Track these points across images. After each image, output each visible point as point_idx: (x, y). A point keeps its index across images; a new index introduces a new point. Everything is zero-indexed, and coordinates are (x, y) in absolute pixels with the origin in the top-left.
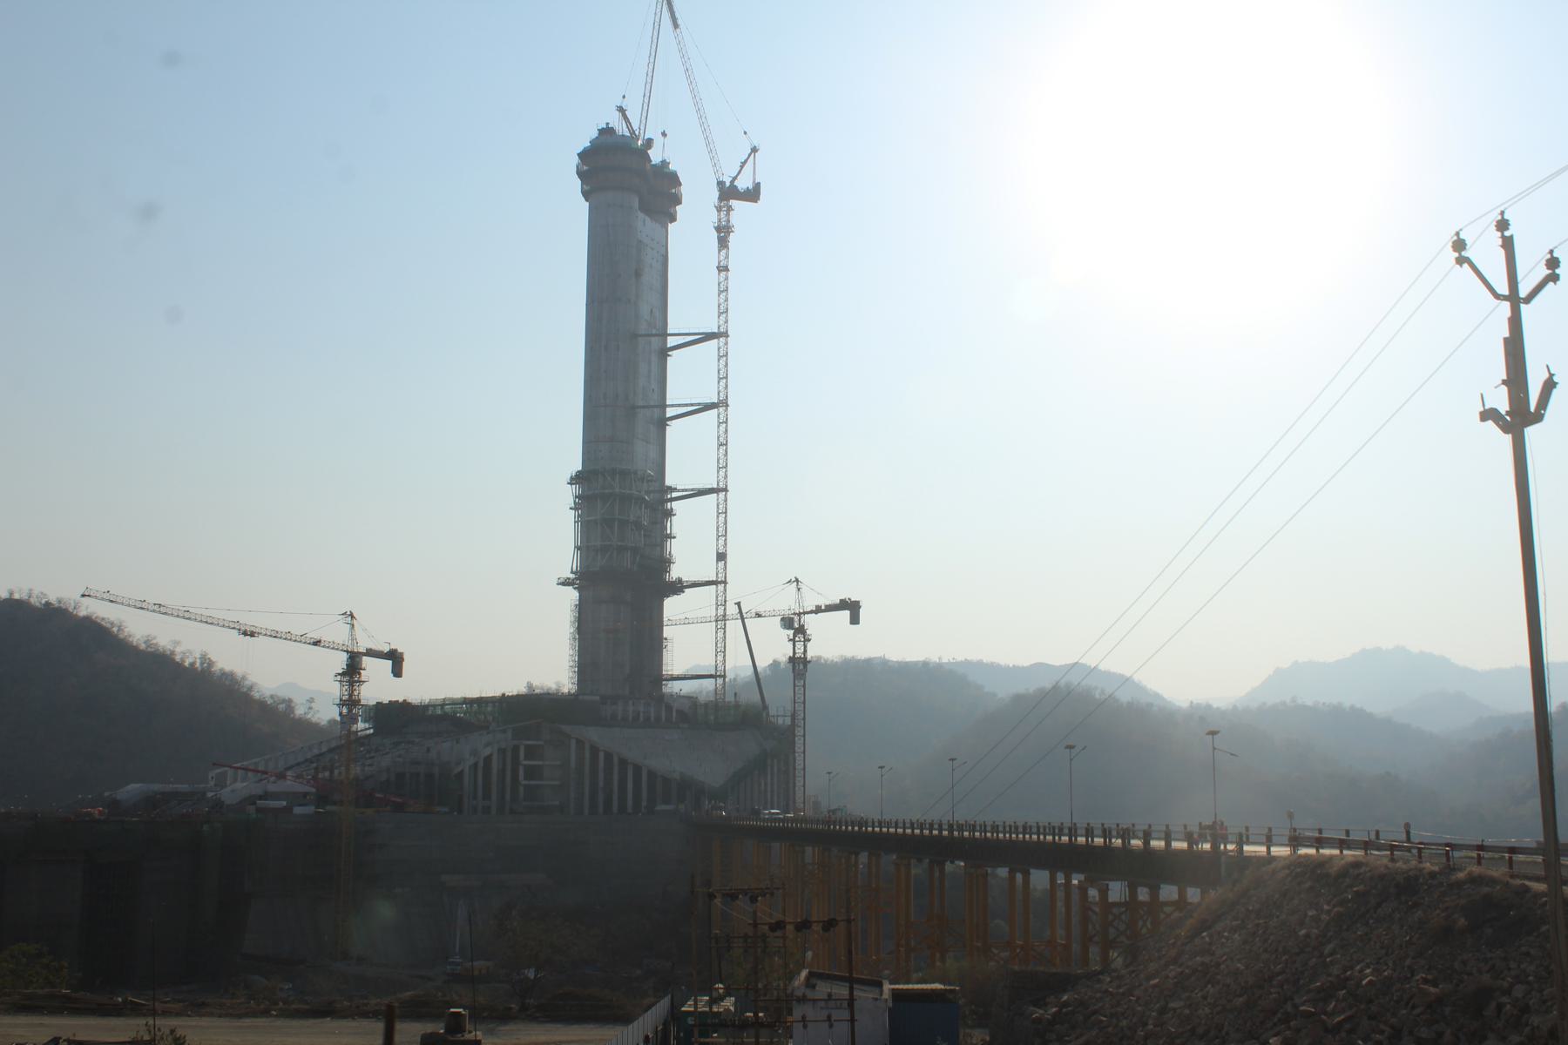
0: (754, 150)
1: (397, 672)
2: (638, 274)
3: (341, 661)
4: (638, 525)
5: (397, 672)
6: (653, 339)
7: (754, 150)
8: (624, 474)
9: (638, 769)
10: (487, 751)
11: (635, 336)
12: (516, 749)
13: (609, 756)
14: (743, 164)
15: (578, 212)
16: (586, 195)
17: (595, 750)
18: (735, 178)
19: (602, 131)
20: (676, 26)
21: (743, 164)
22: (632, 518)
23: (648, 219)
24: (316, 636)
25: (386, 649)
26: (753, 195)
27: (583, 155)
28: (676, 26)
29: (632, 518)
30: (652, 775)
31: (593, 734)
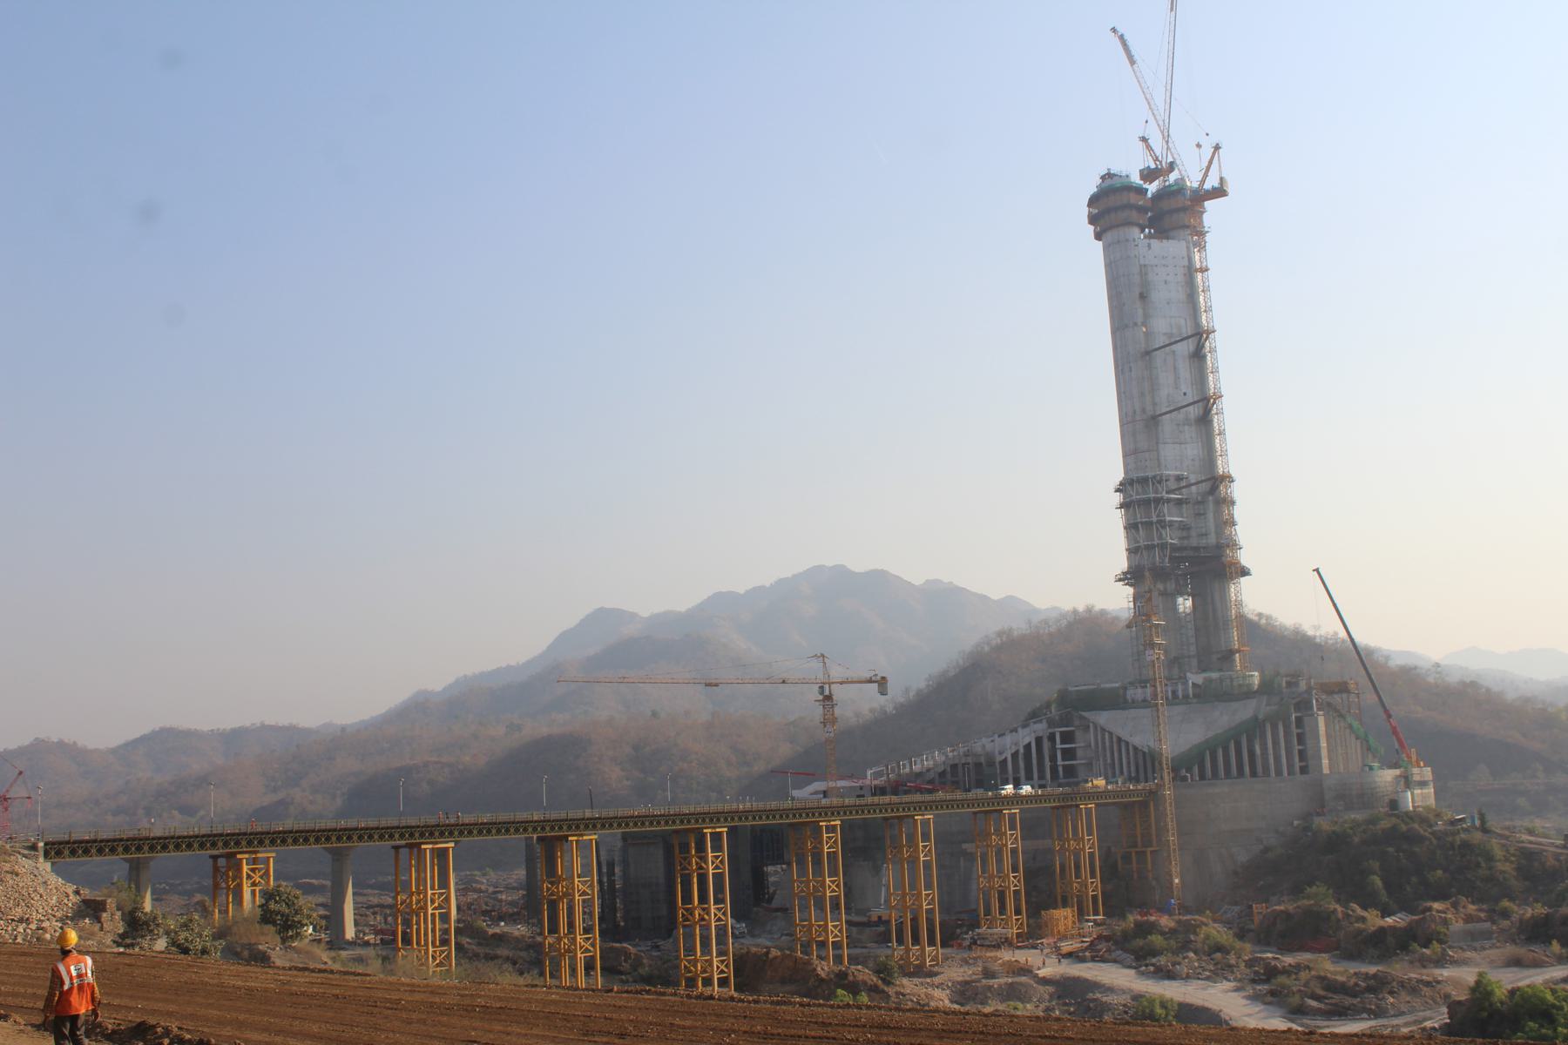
0: (1217, 148)
1: (883, 692)
2: (1143, 297)
3: (816, 688)
4: (1162, 524)
5: (883, 692)
6: (1174, 347)
7: (1217, 148)
8: (1143, 481)
9: (1127, 743)
10: (1026, 741)
11: (1148, 353)
12: (1052, 738)
13: (1111, 734)
14: (1210, 162)
15: (1091, 254)
16: (1098, 237)
17: (1103, 730)
18: (1203, 181)
19: (1103, 178)
20: (1132, 62)
21: (1210, 162)
22: (1155, 519)
23: (1154, 242)
24: (784, 676)
25: (868, 675)
26: (1219, 192)
27: (1093, 201)
28: (1132, 62)
29: (1155, 519)
30: (1135, 749)
31: (1103, 718)
